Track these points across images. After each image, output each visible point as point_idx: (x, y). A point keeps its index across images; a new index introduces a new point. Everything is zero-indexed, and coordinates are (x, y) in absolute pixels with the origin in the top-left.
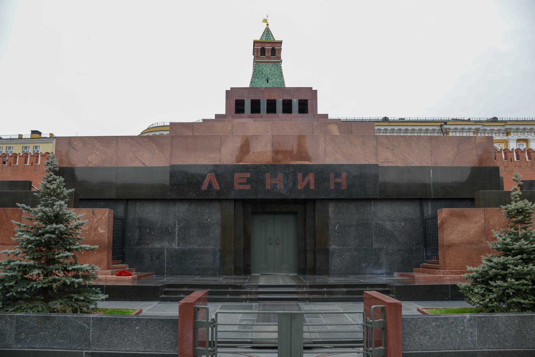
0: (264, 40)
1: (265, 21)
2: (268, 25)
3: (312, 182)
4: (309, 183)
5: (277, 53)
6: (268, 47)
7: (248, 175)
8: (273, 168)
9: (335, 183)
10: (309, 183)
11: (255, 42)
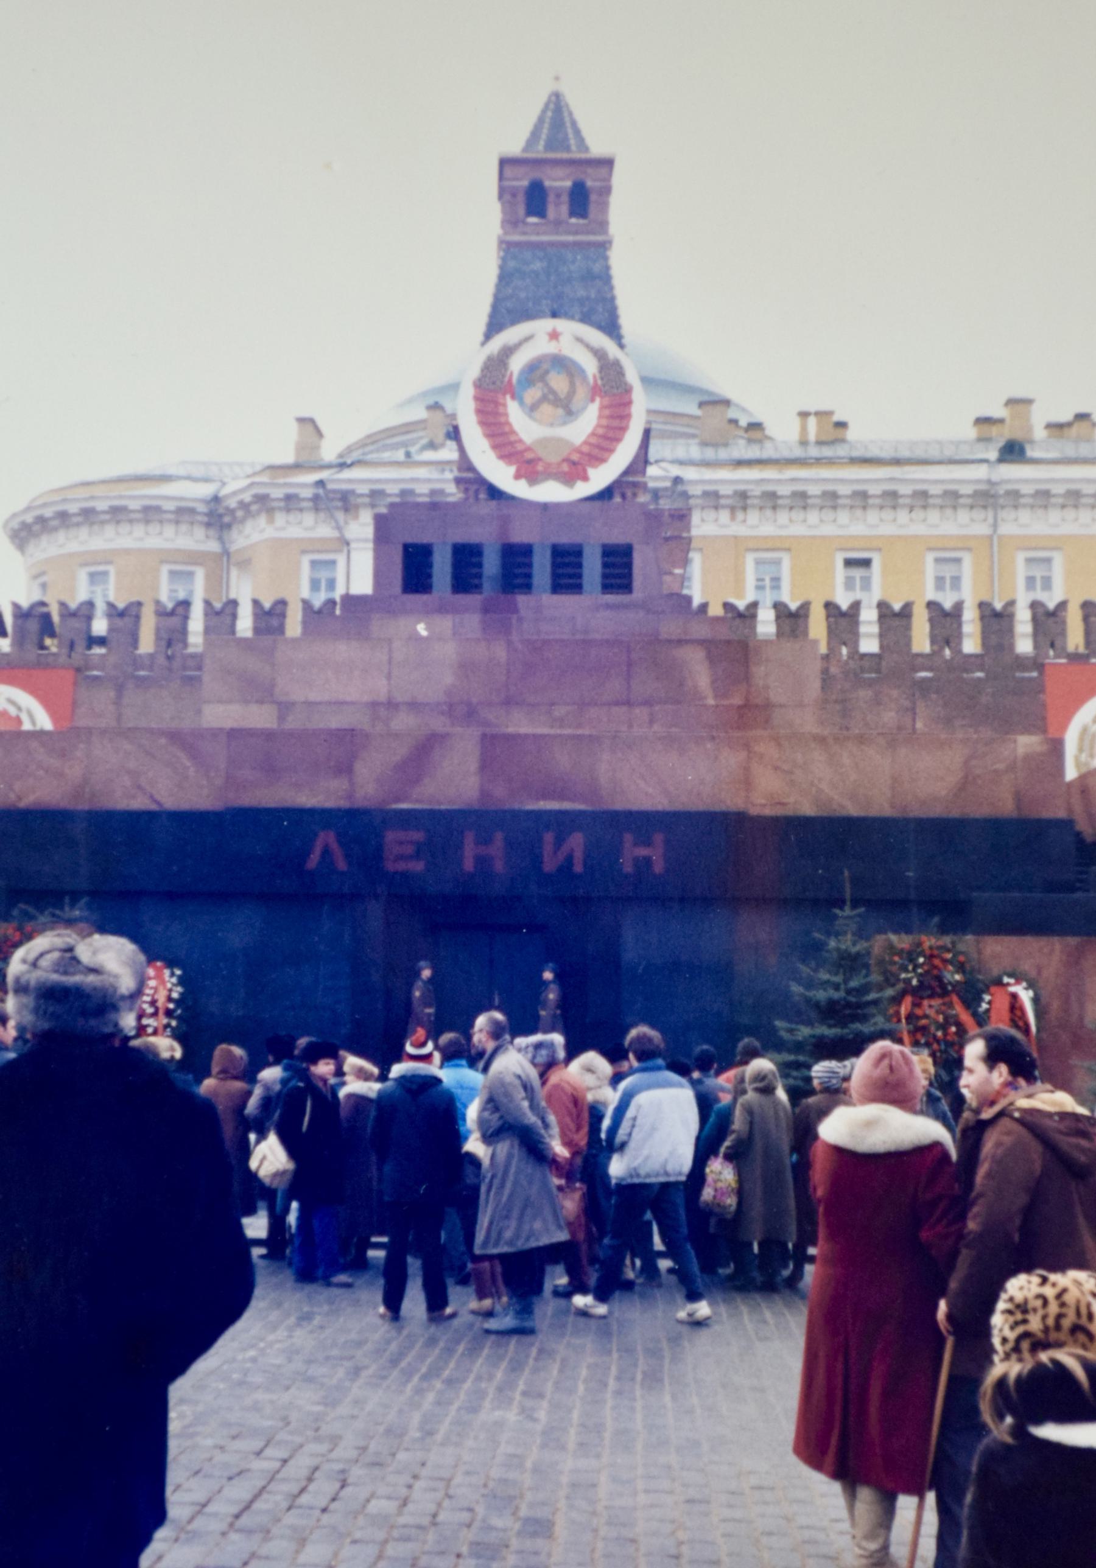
0: (540, 151)
3: (578, 855)
4: (570, 859)
5: (593, 209)
6: (559, 182)
7: (418, 836)
8: (480, 820)
9: (636, 860)
11: (505, 163)
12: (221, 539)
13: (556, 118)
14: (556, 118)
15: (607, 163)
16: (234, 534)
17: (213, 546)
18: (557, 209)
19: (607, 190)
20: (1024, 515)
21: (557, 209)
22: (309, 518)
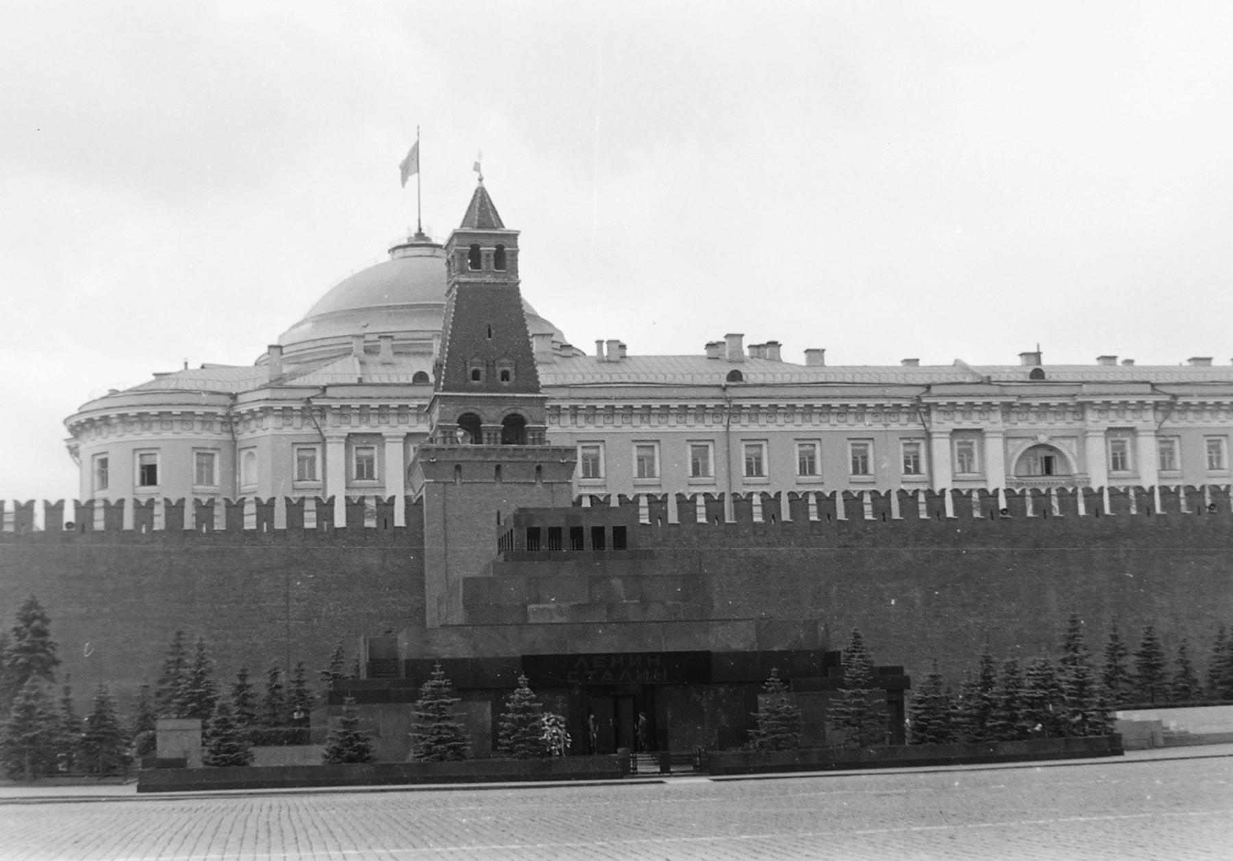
1: (477, 167)
2: (481, 180)
5: (508, 263)
6: (488, 249)
13: (482, 208)
15: (514, 236)
16: (240, 428)
18: (488, 264)
19: (515, 254)
21: (488, 264)
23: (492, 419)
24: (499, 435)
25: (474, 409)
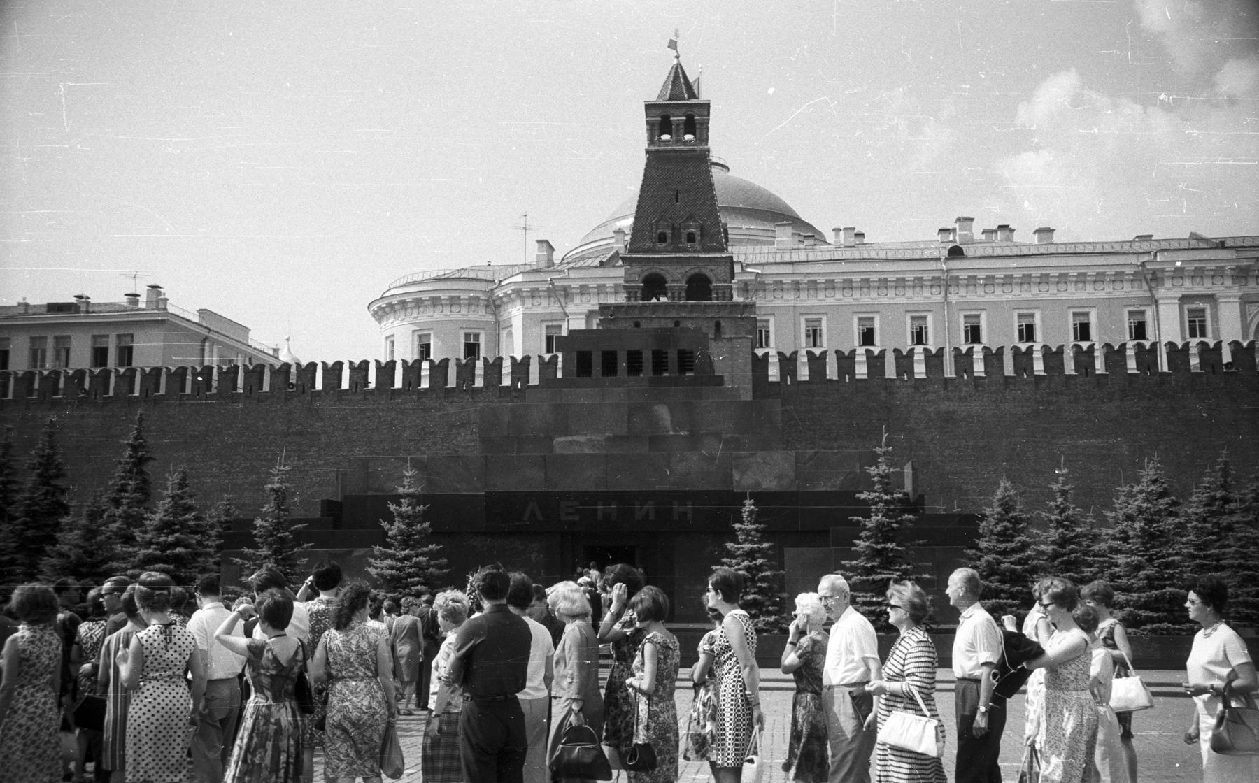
1: (673, 45)
4: (647, 514)
8: (607, 497)
10: (647, 514)
12: (495, 314)
13: (680, 82)
14: (680, 82)
17: (490, 318)
20: (962, 291)
22: (545, 303)
23: (676, 277)
24: (683, 294)
25: (658, 269)
